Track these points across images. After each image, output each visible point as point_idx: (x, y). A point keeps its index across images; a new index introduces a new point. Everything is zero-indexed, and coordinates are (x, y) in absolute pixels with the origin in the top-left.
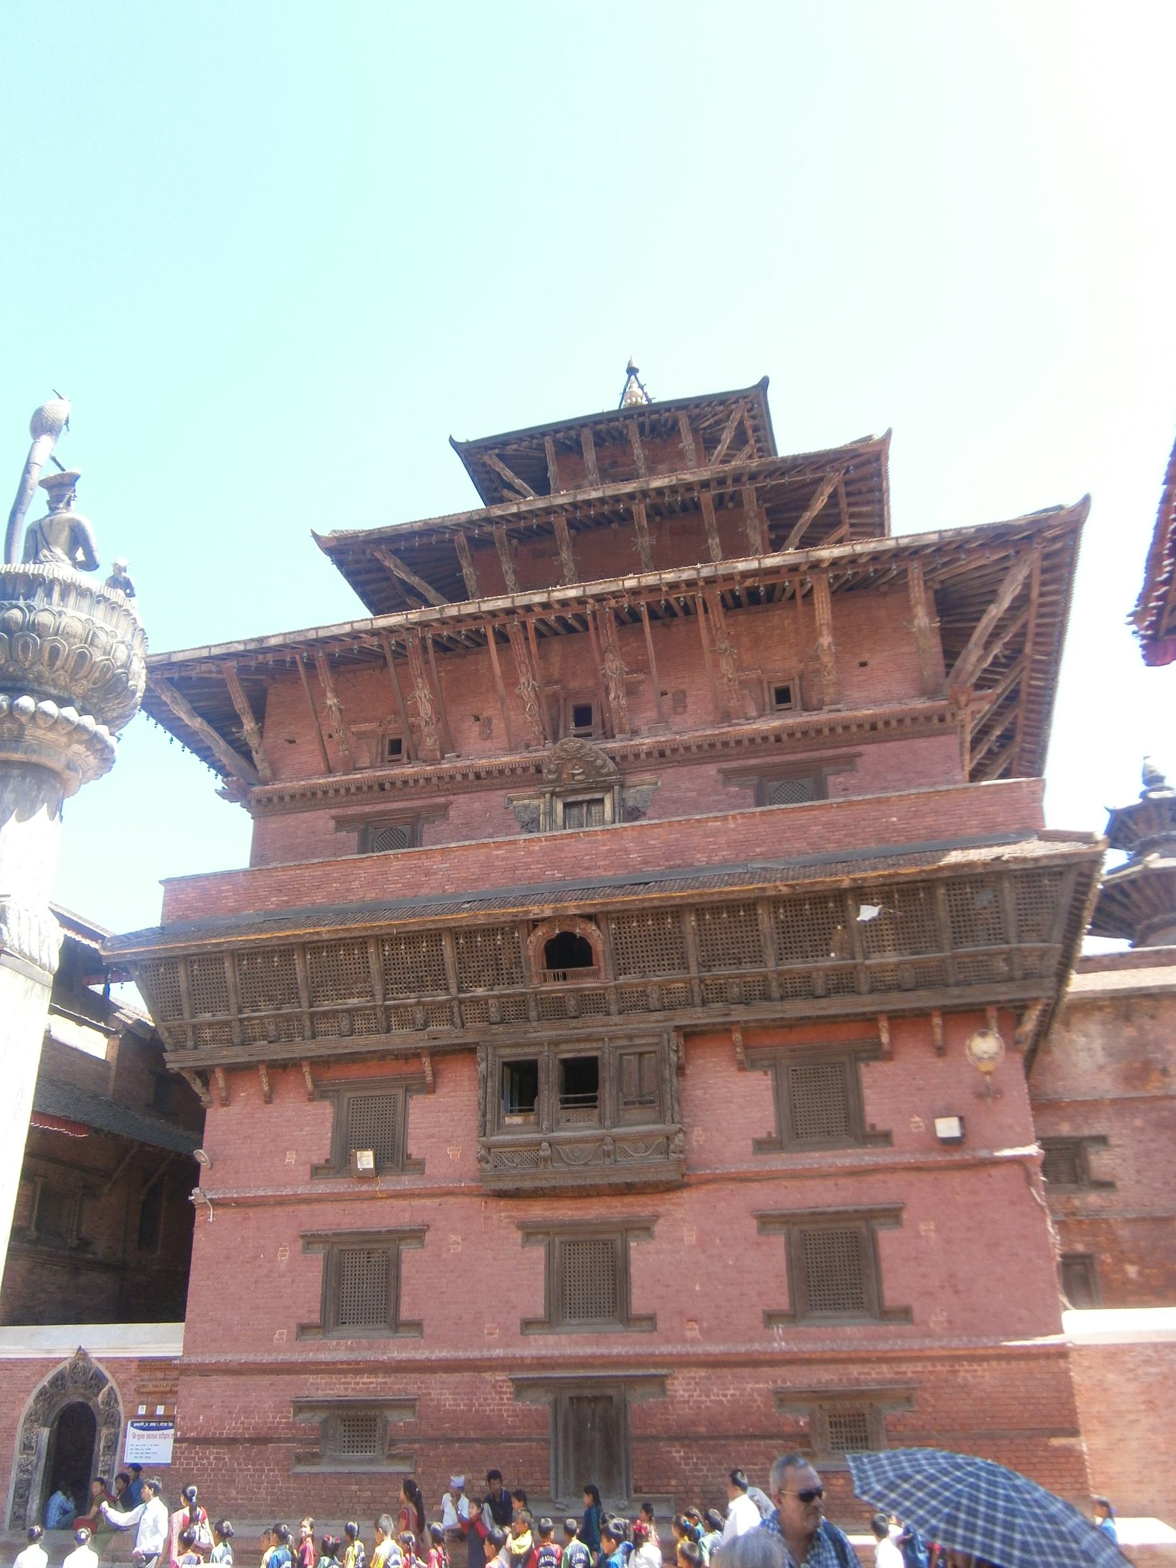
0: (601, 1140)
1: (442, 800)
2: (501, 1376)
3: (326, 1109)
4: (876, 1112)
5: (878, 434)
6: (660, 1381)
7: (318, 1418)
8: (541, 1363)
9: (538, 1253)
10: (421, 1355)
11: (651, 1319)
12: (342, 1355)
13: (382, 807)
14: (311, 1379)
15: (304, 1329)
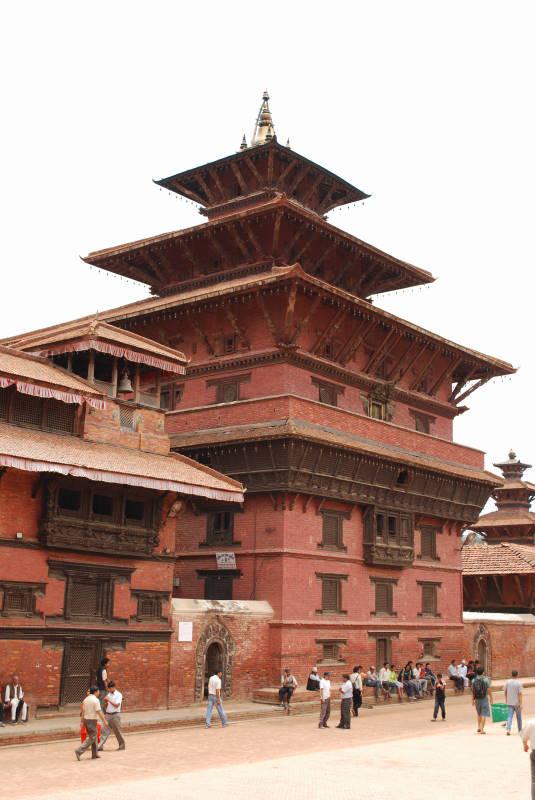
0: (398, 550)
1: (341, 384)
2: (365, 632)
3: (319, 520)
4: (440, 550)
5: (434, 276)
6: (397, 634)
7: (321, 646)
8: (375, 627)
9: (374, 587)
10: (346, 623)
11: (396, 614)
12: (328, 623)
13: (324, 379)
14: (320, 631)
15: (317, 611)
